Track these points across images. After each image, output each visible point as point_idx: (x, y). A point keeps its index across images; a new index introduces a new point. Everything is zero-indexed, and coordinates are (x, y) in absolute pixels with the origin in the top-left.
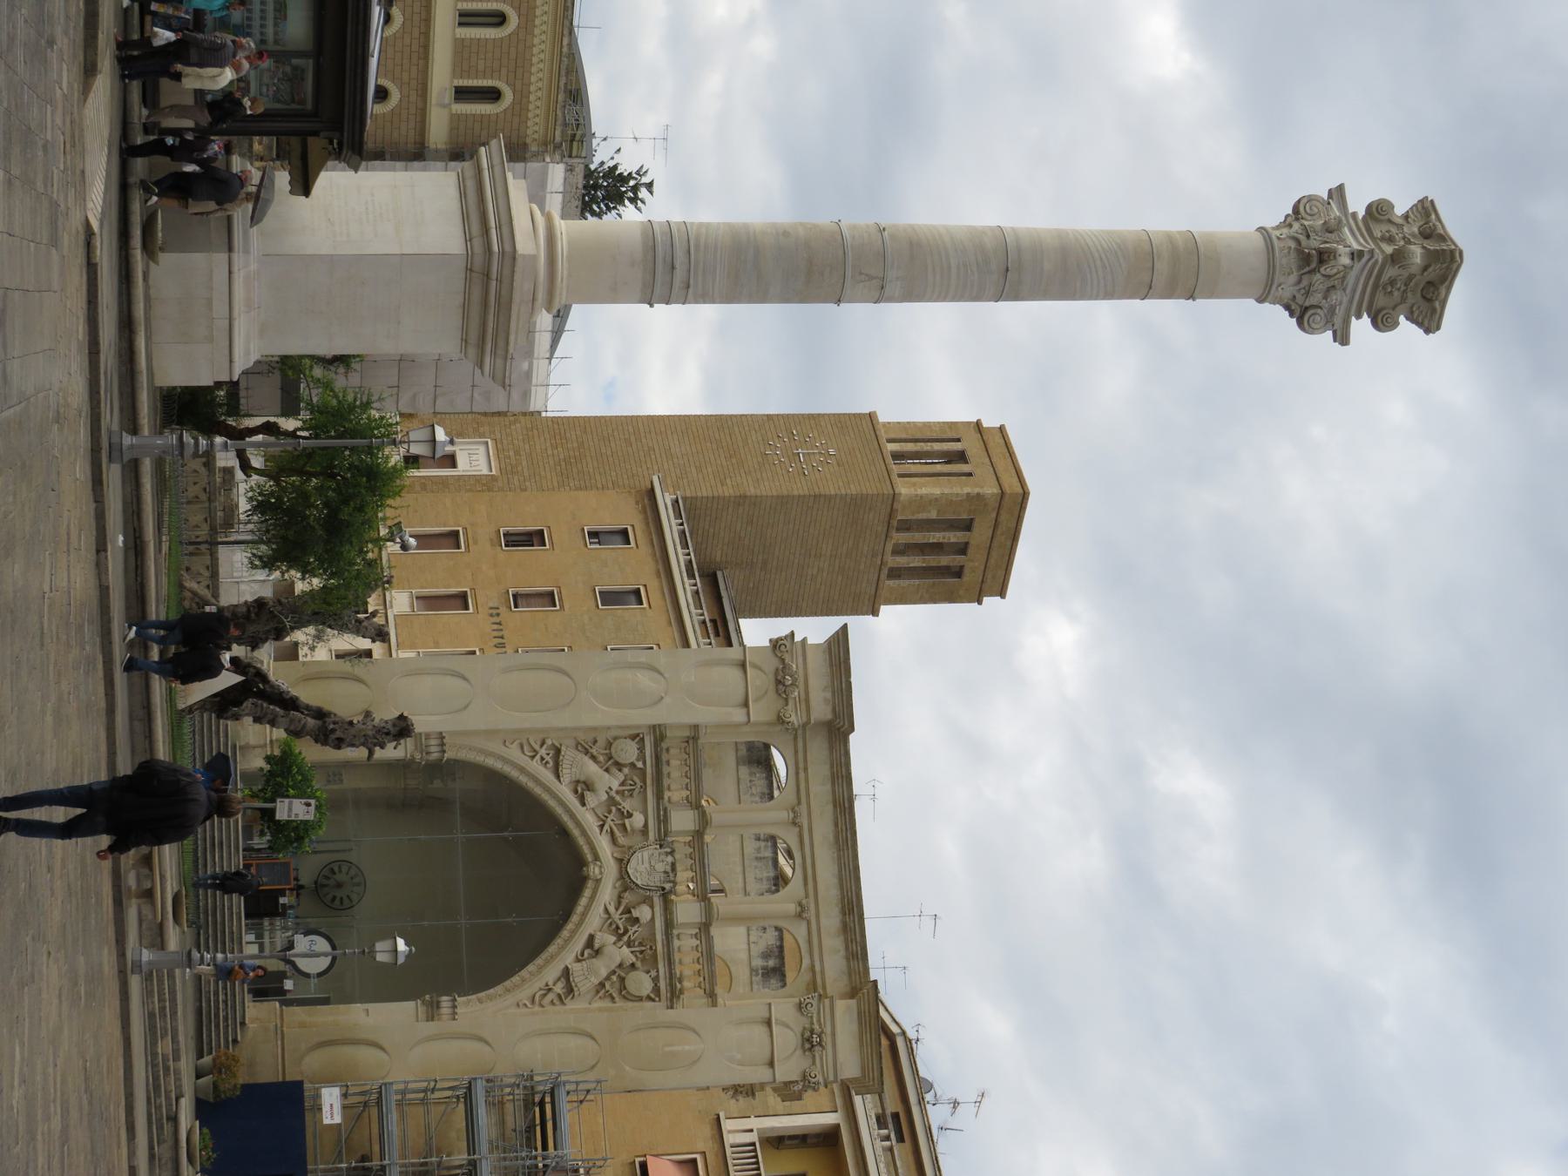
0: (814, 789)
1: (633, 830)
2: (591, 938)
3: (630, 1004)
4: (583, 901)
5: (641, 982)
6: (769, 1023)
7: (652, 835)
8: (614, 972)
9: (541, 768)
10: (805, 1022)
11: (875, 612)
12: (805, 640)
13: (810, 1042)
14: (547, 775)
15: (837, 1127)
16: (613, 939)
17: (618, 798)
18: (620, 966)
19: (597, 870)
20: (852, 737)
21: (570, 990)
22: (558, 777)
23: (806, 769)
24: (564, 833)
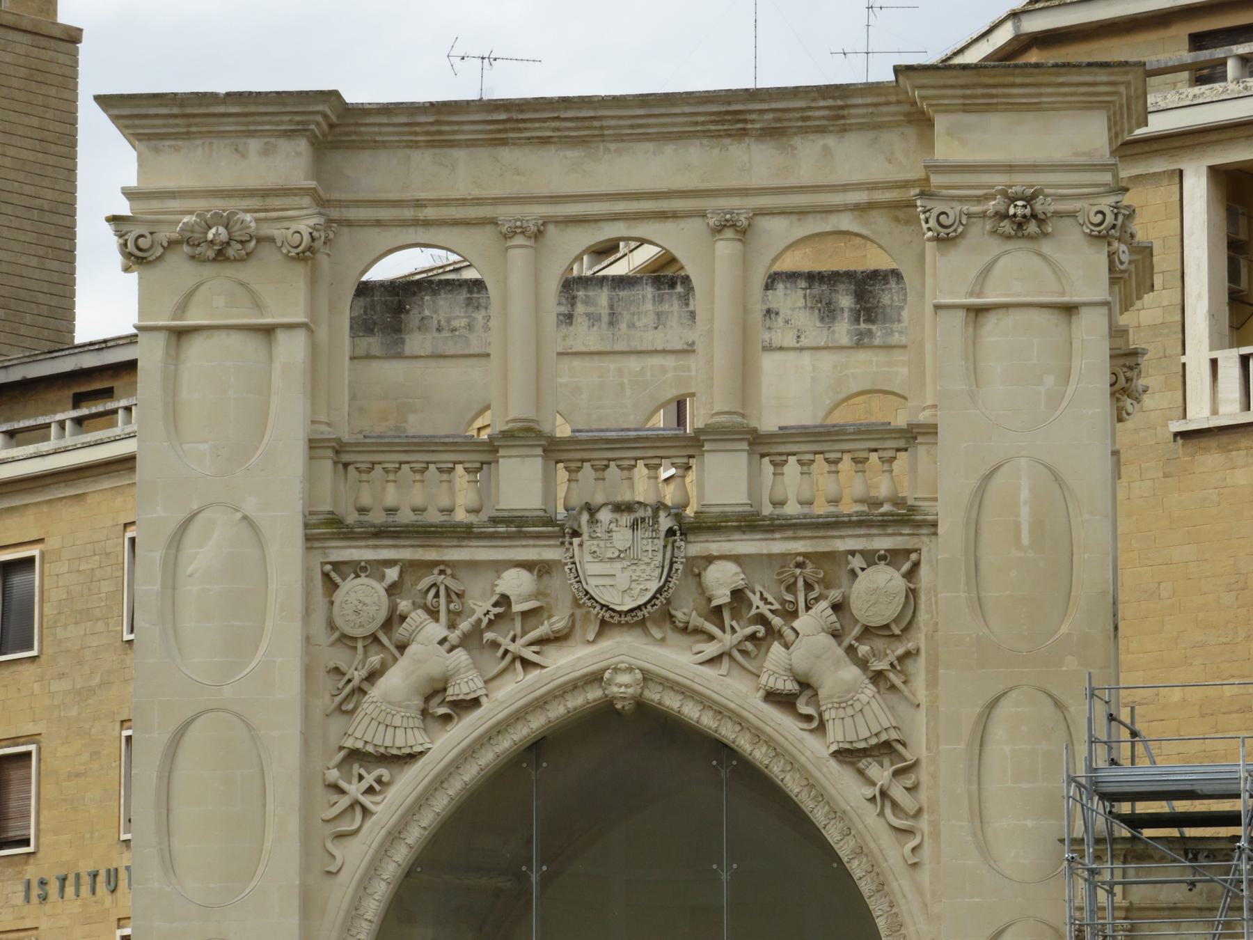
0: (462, 186)
1: (538, 595)
2: (772, 697)
3: (923, 616)
4: (691, 712)
5: (876, 591)
6: (978, 312)
7: (550, 553)
8: (851, 650)
9: (392, 792)
10: (979, 231)
11: (72, 37)
12: (129, 194)
13: (1024, 220)
14: (407, 783)
15: (1214, 171)
16: (776, 647)
17: (465, 625)
18: (836, 635)
19: (624, 678)
20: (350, 97)
21: (886, 749)
22: (412, 757)
23: (419, 204)
24: (537, 748)
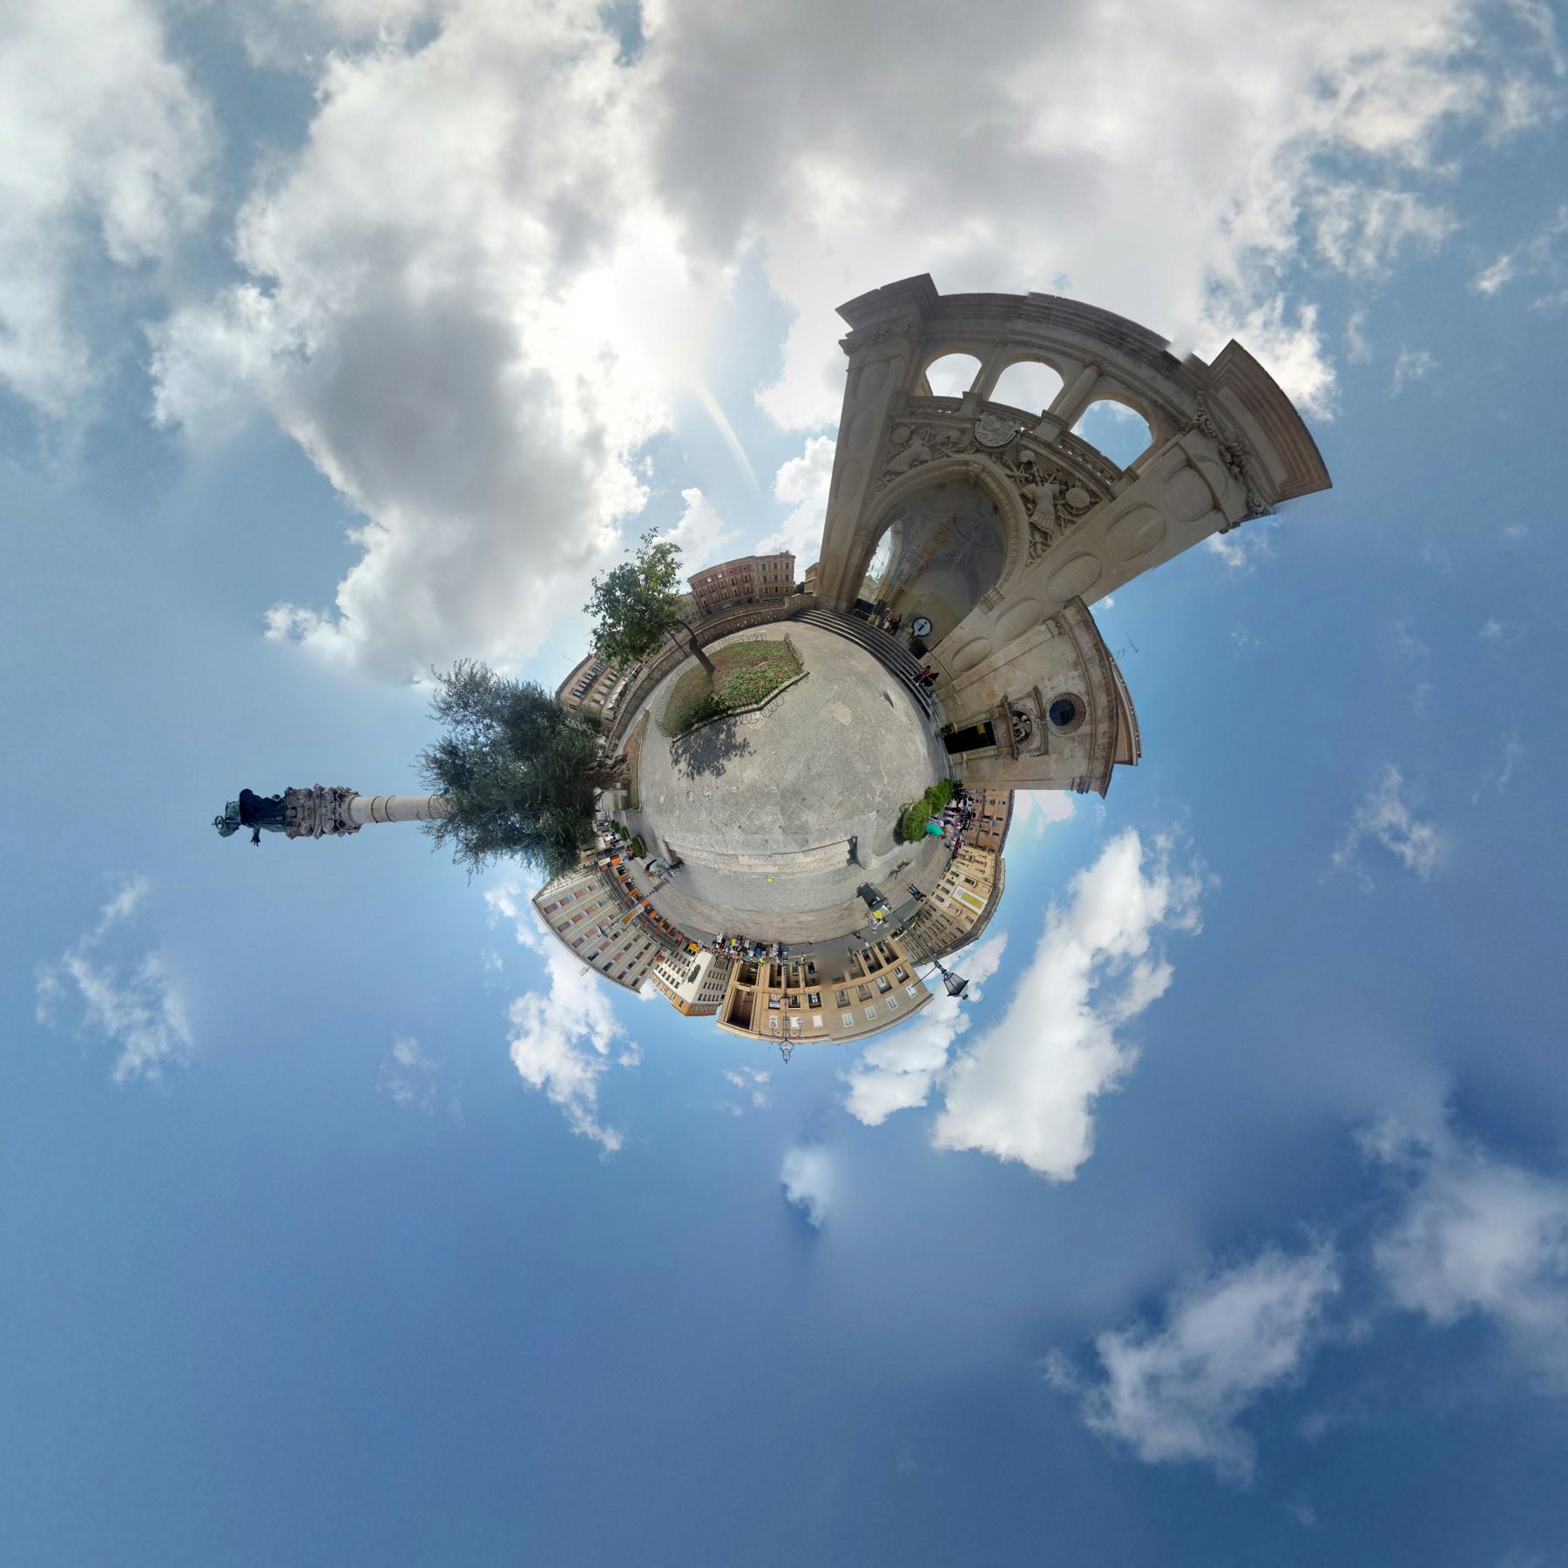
5: (1078, 496)
